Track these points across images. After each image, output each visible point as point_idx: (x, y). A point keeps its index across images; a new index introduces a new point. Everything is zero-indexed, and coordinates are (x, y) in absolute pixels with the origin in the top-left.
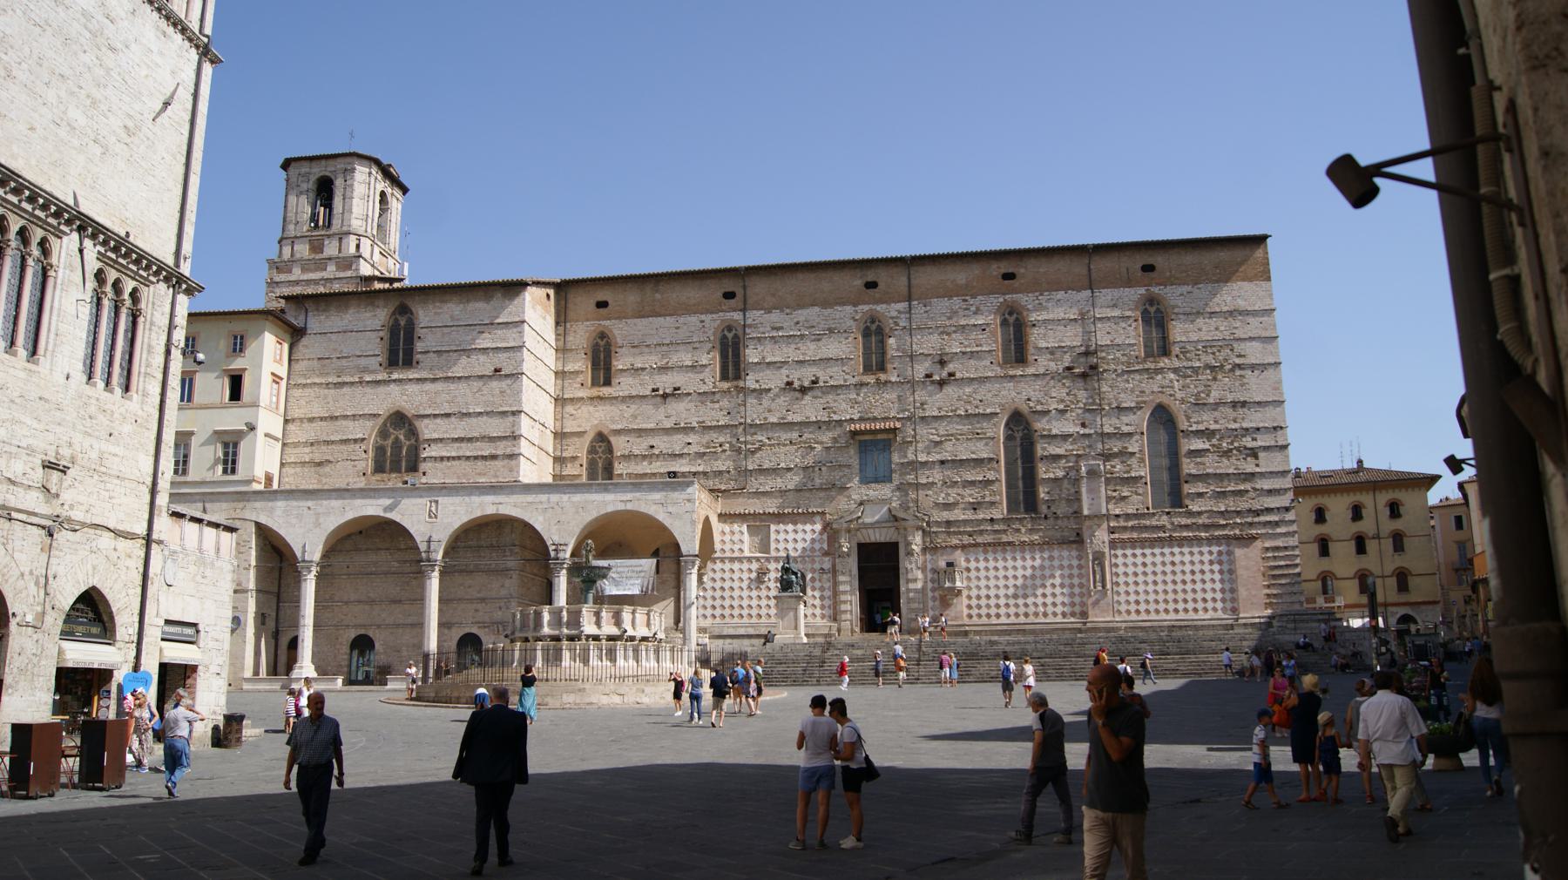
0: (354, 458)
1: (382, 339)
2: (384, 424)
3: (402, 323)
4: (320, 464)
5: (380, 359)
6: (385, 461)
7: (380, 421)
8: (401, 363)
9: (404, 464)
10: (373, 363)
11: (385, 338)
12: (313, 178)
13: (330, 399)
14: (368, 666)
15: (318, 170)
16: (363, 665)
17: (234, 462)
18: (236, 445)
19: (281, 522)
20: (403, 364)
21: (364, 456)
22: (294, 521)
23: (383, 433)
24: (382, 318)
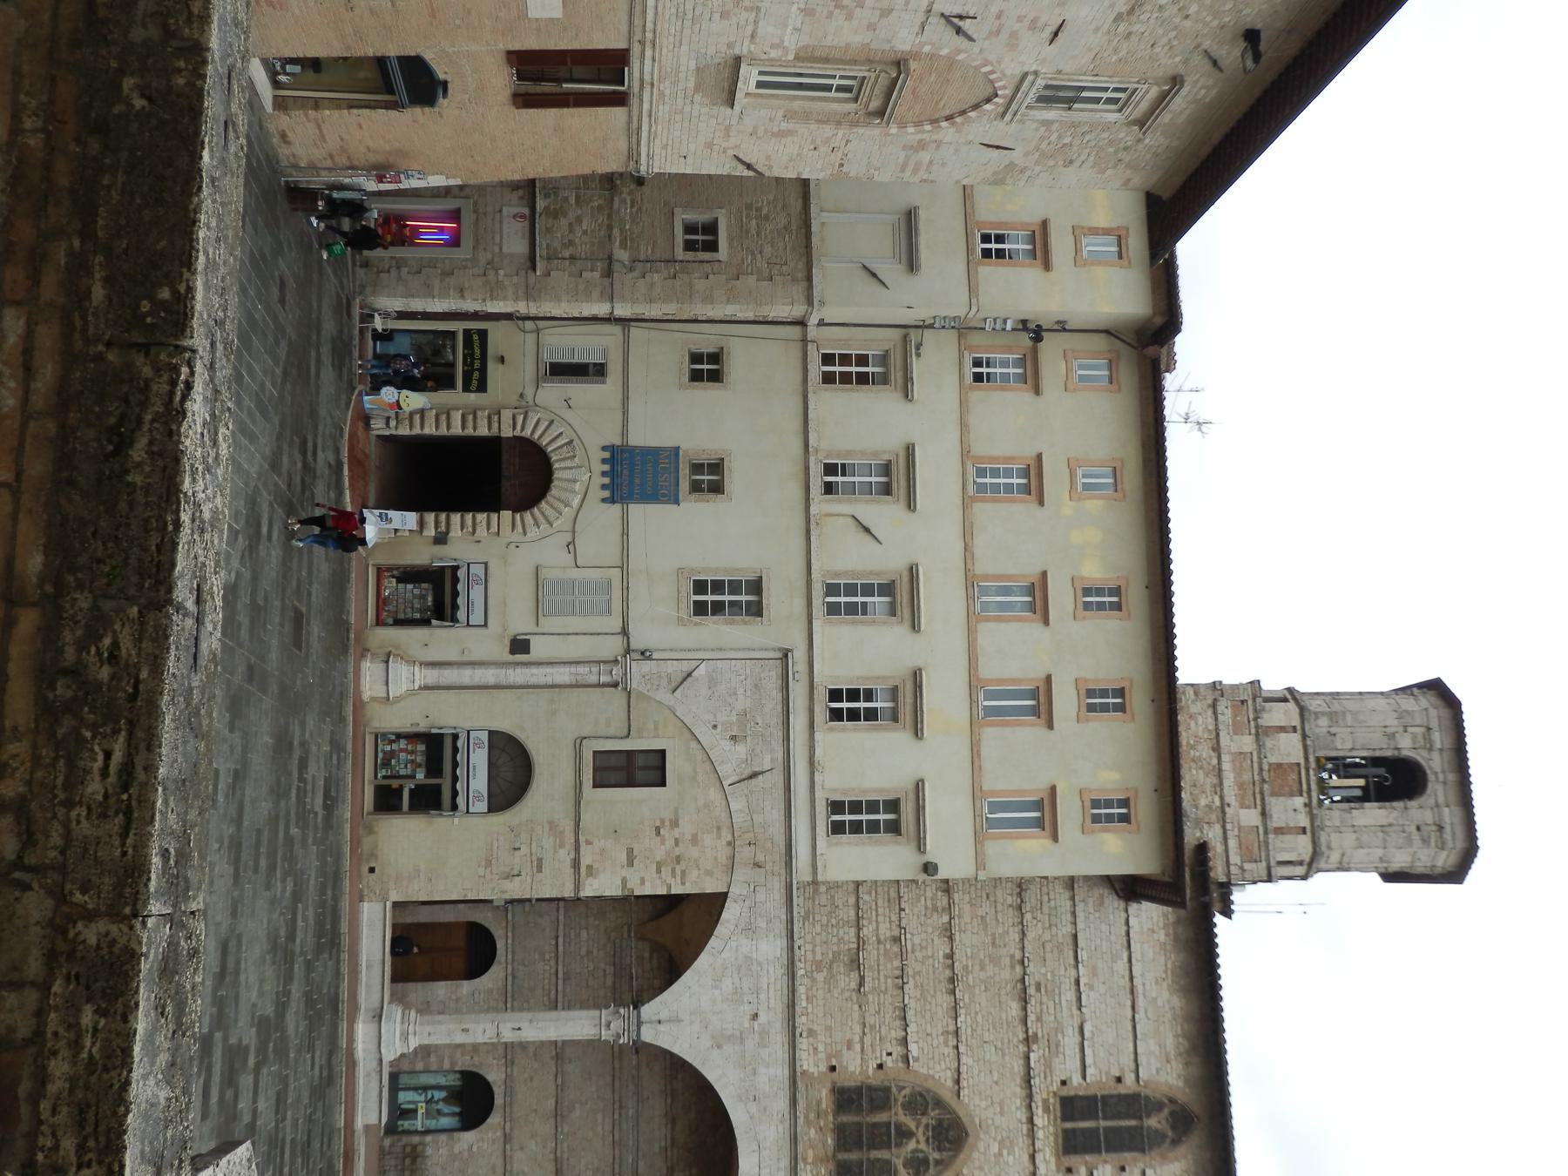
0: (867, 1040)
1: (1119, 1080)
2: (939, 1103)
3: (1153, 1122)
4: (855, 963)
5: (1076, 1079)
6: (859, 1110)
7: (947, 1096)
8: (1069, 1125)
9: (853, 1156)
10: (1068, 1066)
11: (1122, 1090)
12: (1420, 756)
13: (990, 970)
14: (428, 1114)
15: (1435, 764)
16: (429, 1102)
17: (856, 828)
18: (894, 828)
19: (726, 954)
20: (1065, 1131)
21: (873, 1064)
22: (727, 984)
23: (921, 1101)
24: (1163, 1078)
